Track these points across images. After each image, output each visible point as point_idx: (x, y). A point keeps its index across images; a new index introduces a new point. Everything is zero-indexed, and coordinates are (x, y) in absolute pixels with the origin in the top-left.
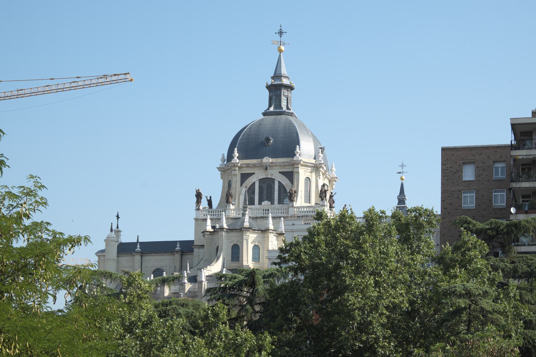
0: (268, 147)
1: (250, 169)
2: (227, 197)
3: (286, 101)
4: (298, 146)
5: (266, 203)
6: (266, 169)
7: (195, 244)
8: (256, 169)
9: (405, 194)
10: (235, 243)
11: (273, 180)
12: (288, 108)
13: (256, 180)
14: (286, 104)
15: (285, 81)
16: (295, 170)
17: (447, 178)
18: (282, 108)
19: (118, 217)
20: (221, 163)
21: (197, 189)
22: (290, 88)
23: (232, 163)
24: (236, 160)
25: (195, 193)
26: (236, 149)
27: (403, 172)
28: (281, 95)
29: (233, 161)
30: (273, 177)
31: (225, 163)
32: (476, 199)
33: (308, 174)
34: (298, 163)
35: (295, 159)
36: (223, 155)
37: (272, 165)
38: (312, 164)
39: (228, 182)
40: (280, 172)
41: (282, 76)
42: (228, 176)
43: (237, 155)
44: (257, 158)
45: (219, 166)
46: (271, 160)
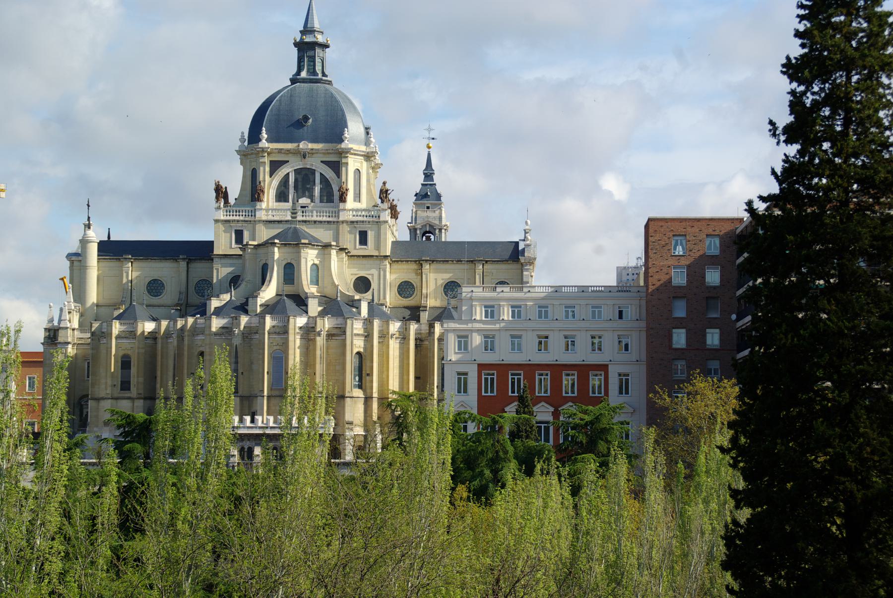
0: (305, 128)
1: (283, 155)
2: (254, 192)
3: (321, 64)
4: (346, 129)
5: (304, 201)
6: (304, 157)
7: (215, 253)
8: (290, 155)
9: (434, 167)
10: (289, 262)
11: (313, 172)
12: (324, 75)
13: (290, 170)
14: (321, 68)
15: (320, 39)
16: (344, 161)
17: (655, 252)
18: (317, 75)
19: (88, 206)
20: (240, 144)
21: (217, 181)
22: (325, 46)
23: (260, 148)
24: (264, 144)
25: (214, 186)
26: (264, 128)
27: (429, 138)
28: (315, 56)
29: (261, 145)
30: (314, 168)
31: (246, 144)
32: (687, 275)
33: (358, 165)
34: (347, 151)
35: (343, 146)
36: (243, 133)
37: (312, 152)
38: (363, 151)
39: (251, 170)
40: (322, 162)
41: (315, 31)
42: (251, 162)
43: (266, 136)
44: (291, 142)
45: (237, 149)
46: (311, 146)
